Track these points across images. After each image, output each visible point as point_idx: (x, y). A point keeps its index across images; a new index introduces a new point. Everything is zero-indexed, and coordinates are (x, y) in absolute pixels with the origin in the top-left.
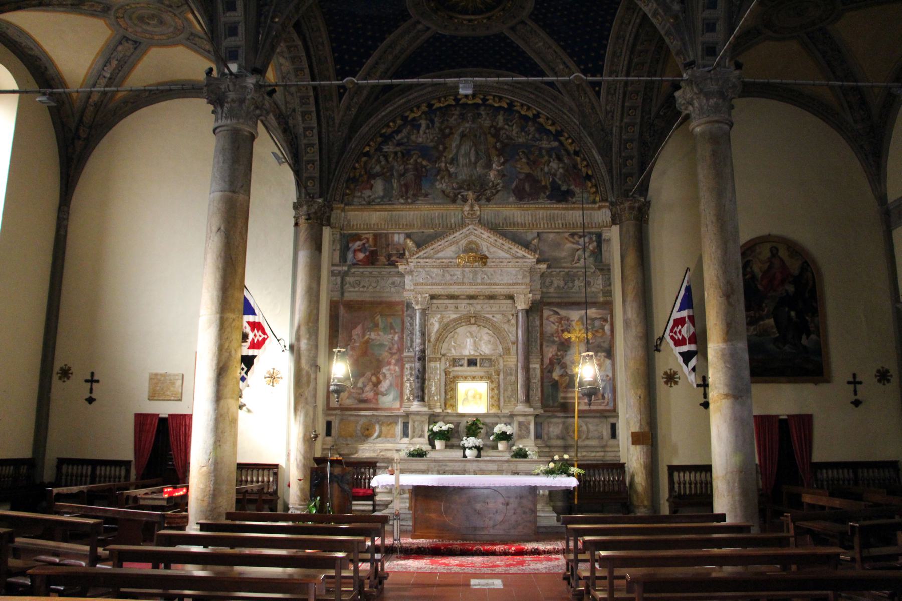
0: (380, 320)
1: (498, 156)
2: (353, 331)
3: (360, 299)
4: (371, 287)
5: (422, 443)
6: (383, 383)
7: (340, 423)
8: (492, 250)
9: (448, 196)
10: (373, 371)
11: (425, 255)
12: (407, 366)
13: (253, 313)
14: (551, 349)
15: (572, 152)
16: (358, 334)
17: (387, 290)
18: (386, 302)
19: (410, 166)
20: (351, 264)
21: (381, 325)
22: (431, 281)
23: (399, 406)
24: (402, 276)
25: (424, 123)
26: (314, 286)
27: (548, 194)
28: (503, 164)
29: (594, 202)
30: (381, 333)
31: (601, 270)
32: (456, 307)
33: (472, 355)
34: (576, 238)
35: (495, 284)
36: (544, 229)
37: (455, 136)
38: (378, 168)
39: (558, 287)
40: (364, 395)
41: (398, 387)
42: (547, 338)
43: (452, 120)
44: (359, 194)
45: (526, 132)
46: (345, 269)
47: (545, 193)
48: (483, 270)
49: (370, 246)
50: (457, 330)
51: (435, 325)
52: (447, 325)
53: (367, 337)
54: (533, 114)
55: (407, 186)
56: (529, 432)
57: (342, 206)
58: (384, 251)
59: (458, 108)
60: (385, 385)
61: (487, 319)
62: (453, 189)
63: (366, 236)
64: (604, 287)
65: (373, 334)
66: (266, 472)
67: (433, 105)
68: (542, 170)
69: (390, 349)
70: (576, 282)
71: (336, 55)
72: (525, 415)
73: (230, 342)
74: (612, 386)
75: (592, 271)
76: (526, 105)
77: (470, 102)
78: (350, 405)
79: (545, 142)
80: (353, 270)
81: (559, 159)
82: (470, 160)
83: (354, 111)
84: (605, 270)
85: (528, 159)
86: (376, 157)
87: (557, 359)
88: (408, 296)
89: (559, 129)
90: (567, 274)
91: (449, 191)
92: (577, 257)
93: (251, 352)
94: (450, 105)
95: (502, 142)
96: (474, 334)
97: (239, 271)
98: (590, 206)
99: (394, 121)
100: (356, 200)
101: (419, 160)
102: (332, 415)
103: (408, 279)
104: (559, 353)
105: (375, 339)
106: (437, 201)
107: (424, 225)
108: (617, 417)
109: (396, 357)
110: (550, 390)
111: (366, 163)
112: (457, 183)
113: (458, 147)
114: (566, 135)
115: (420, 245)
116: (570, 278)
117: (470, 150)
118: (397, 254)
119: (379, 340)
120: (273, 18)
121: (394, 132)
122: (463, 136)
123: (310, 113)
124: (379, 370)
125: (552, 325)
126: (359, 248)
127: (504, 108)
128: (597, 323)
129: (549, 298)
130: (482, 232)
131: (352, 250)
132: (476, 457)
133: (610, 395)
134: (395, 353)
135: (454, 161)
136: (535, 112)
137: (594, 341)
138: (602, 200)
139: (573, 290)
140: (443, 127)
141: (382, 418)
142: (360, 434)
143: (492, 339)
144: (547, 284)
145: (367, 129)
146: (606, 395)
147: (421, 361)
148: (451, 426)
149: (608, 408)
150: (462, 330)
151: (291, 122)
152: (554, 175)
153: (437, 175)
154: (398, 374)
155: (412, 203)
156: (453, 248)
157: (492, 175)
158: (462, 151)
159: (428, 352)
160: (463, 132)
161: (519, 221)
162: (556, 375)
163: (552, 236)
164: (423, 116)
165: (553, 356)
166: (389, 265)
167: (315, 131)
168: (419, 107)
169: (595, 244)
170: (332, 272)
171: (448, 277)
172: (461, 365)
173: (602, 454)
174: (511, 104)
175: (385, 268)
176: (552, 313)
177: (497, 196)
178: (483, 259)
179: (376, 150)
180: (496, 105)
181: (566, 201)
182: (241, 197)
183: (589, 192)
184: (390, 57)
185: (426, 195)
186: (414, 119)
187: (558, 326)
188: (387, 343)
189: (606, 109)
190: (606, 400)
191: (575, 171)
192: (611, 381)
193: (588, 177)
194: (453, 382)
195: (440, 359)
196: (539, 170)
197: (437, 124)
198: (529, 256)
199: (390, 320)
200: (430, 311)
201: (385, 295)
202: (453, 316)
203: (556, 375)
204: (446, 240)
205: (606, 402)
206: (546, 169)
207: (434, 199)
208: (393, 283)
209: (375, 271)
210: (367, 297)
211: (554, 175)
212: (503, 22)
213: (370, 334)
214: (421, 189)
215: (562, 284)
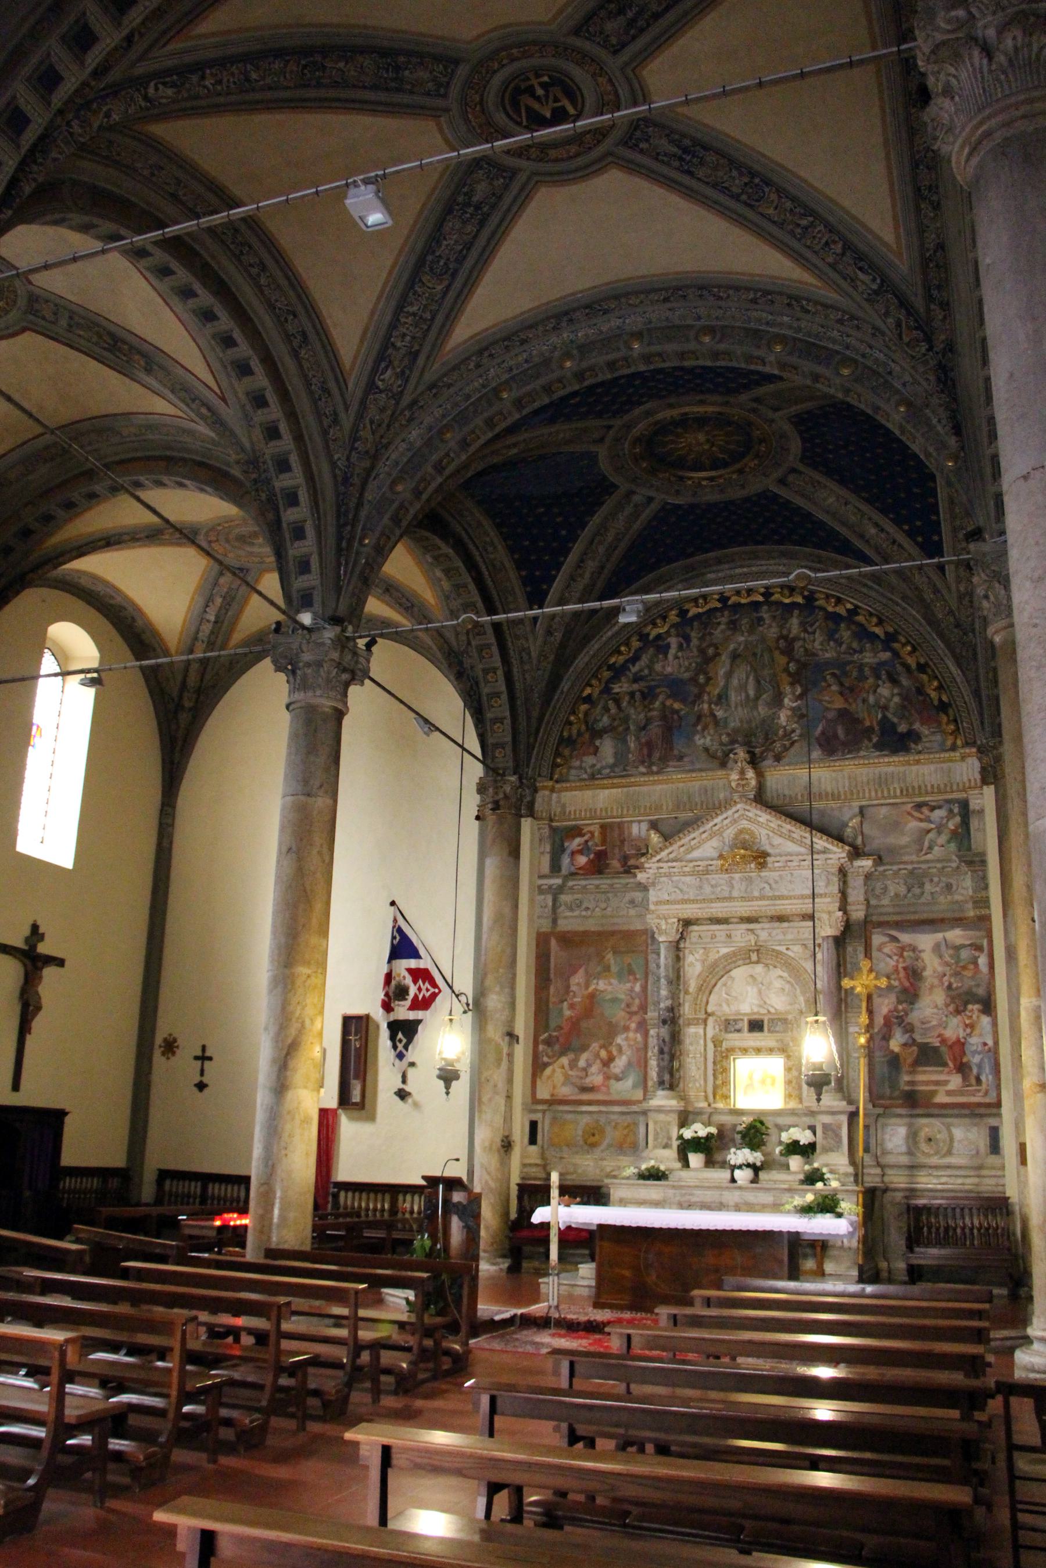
0: (612, 962)
1: (792, 684)
3: (581, 929)
5: (665, 1158)
7: (552, 1124)
8: (777, 840)
9: (713, 756)
10: (602, 1042)
11: (671, 856)
12: (652, 1032)
13: (416, 955)
14: (886, 1001)
15: (914, 666)
16: (578, 984)
18: (620, 932)
19: (655, 713)
21: (614, 969)
22: (680, 897)
24: (644, 888)
25: (673, 641)
26: (507, 910)
27: (875, 740)
28: (800, 697)
29: (954, 748)
30: (614, 981)
31: (970, 863)
32: (729, 936)
33: (758, 1013)
34: (925, 810)
35: (780, 897)
36: (870, 799)
37: (723, 657)
38: (605, 720)
39: (897, 895)
43: (718, 633)
44: (577, 763)
45: (836, 641)
46: (558, 881)
47: (870, 740)
48: (763, 874)
50: (733, 973)
51: (694, 965)
52: (715, 965)
53: (592, 988)
54: (848, 610)
55: (649, 745)
56: (840, 1141)
57: (550, 783)
58: (617, 851)
59: (726, 613)
60: (619, 1064)
61: (779, 953)
62: (722, 744)
64: (974, 891)
66: (372, 1195)
67: (688, 611)
68: (864, 701)
69: (628, 1006)
70: (928, 887)
71: (516, 556)
72: (833, 1113)
73: (303, 1009)
75: (954, 865)
76: (833, 596)
77: (743, 601)
79: (868, 654)
80: (570, 883)
81: (894, 681)
82: (747, 696)
83: (558, 636)
84: (976, 862)
85: (841, 684)
86: (602, 702)
88: (652, 921)
89: (890, 630)
90: (912, 872)
91: (714, 748)
92: (926, 844)
93: (412, 1015)
94: (716, 609)
95: (798, 661)
96: (760, 979)
97: (318, 906)
98: (947, 755)
99: (627, 644)
100: (573, 772)
101: (668, 703)
102: (535, 1111)
103: (653, 895)
104: (900, 1007)
106: (698, 766)
107: (678, 806)
108: (999, 1115)
109: (636, 1018)
111: (586, 714)
112: (728, 735)
113: (729, 675)
114: (903, 640)
115: (667, 838)
116: (916, 879)
117: (747, 678)
120: (362, 539)
121: (627, 661)
122: (735, 656)
123: (488, 646)
127: (799, 604)
128: (965, 954)
129: (881, 914)
130: (759, 812)
131: (568, 851)
132: (752, 1182)
134: (636, 1013)
135: (722, 699)
136: (849, 606)
138: (967, 744)
139: (923, 900)
140: (704, 645)
141: (613, 1117)
142: (581, 1143)
143: (787, 987)
144: (878, 891)
145: (586, 659)
146: (983, 1078)
148: (713, 1130)
149: (987, 1100)
150: (740, 973)
151: (467, 662)
152: (885, 708)
153: (695, 725)
154: (641, 1046)
155: (658, 773)
156: (715, 843)
157: (783, 717)
158: (735, 682)
159: (687, 1010)
160: (735, 650)
161: (829, 789)
162: (895, 1045)
163: (884, 810)
164: (672, 630)
167: (500, 673)
168: (664, 618)
169: (958, 819)
170: (539, 887)
171: (708, 889)
172: (739, 1031)
173: (976, 1180)
174: (810, 599)
176: (887, 939)
177: (792, 751)
178: (761, 858)
179: (601, 692)
180: (787, 601)
181: (907, 750)
182: (321, 802)
183: (943, 732)
184: (601, 549)
185: (680, 758)
186: (659, 637)
188: (623, 996)
189: (958, 590)
190: (984, 1087)
191: (921, 698)
193: (943, 707)
194: (727, 1057)
195: (705, 1021)
196: (859, 701)
197: (695, 642)
198: (835, 849)
199: (628, 959)
200: (687, 945)
202: (724, 951)
203: (895, 1045)
204: (702, 830)
206: (871, 699)
207: (692, 763)
209: (604, 882)
210: (591, 925)
211: (885, 708)
212: (764, 474)
214: (671, 749)
215: (902, 890)
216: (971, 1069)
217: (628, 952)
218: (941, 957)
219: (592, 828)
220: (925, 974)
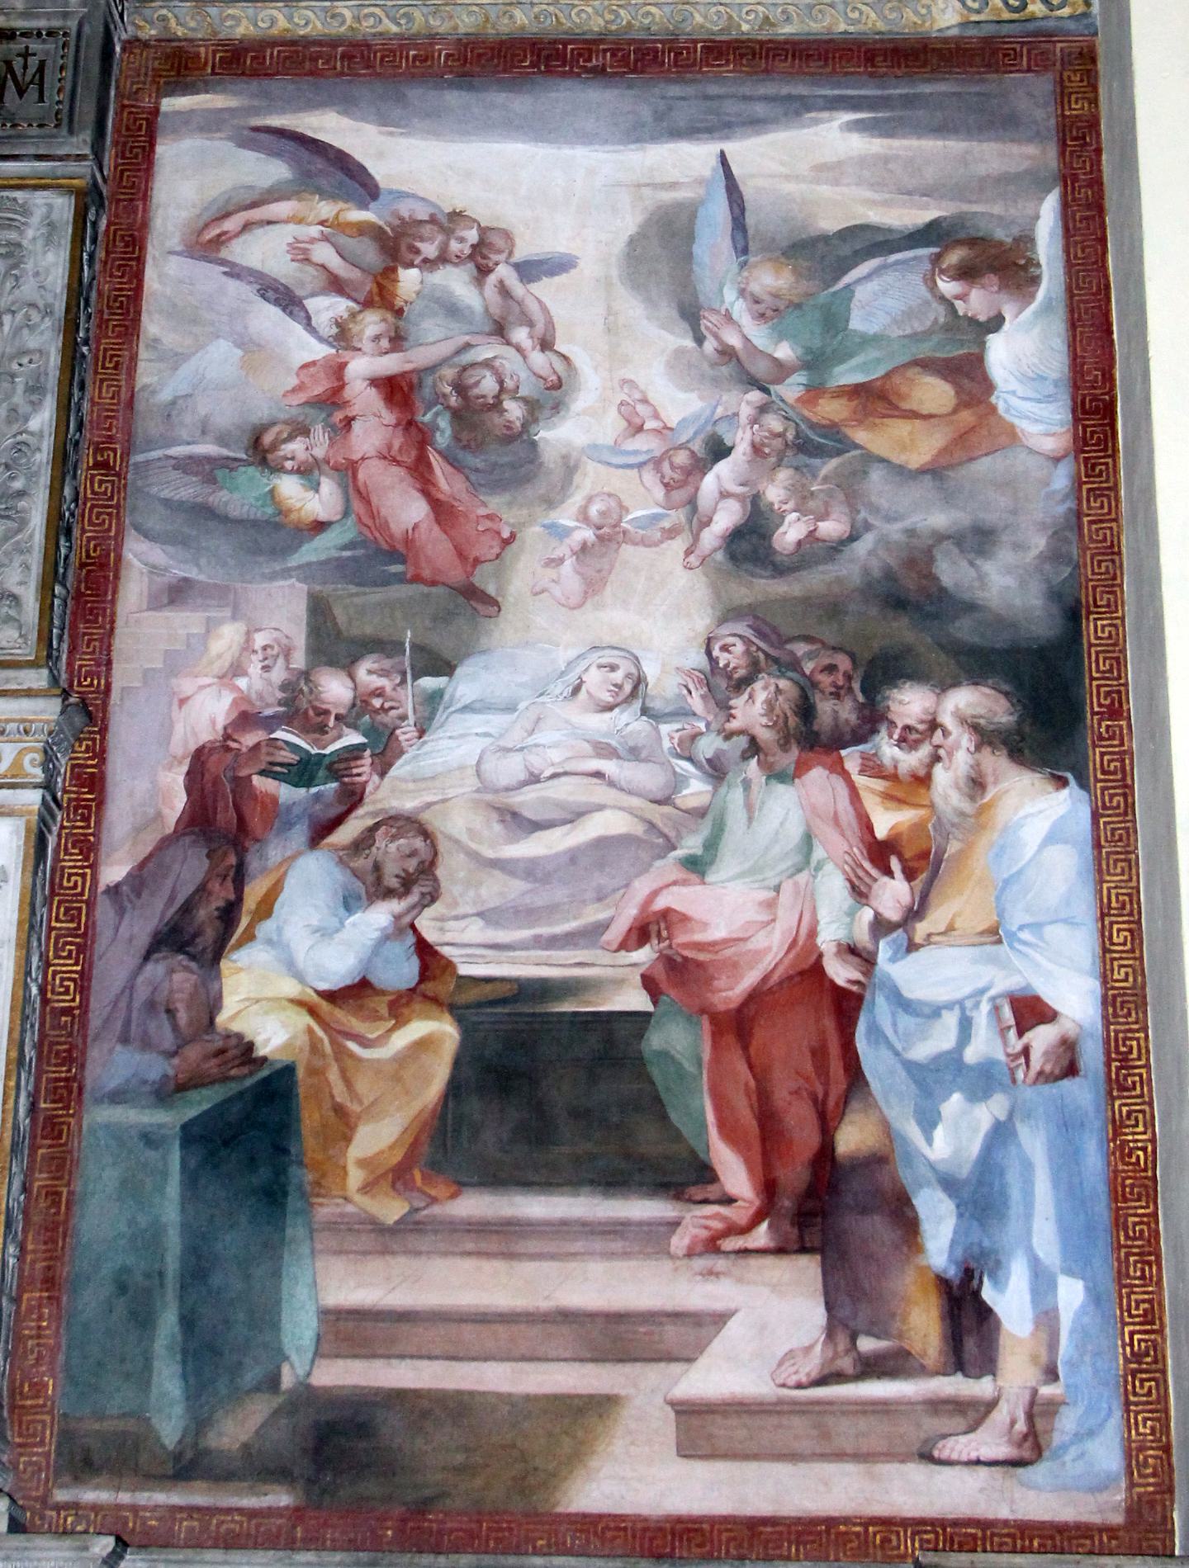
14: (228, 637)
42: (187, 490)
74: (1094, 1159)
87: (303, 771)
104: (335, 689)
110: (169, 1207)
125: (268, 318)
133: (1071, 1294)
137: (831, 528)
165: (245, 719)
176: (275, 170)
187: (343, 336)
192: (1083, 1093)
205: (1010, 1412)
216: (908, 1224)
218: (691, 314)
220: (556, 436)
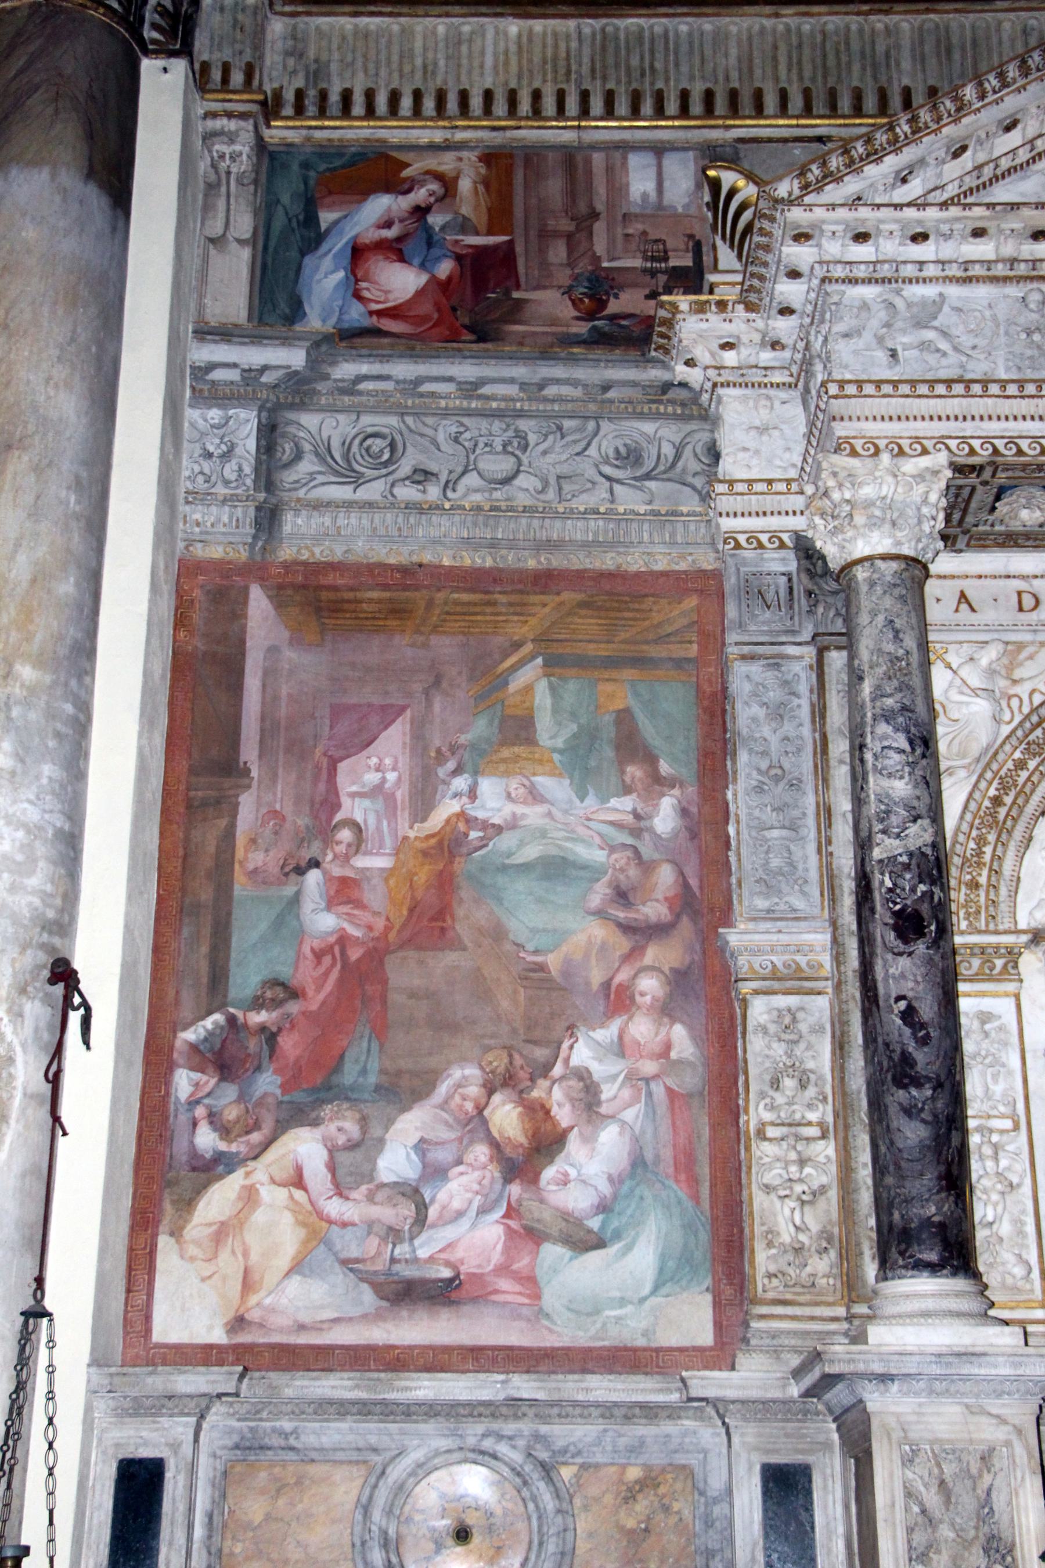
0: (542, 697)
2: (343, 767)
4: (472, 480)
6: (573, 1144)
10: (499, 1061)
16: (377, 790)
17: (580, 503)
20: (329, 328)
23: (706, 1337)
40: (426, 1246)
41: (693, 1181)
46: (295, 358)
49: (465, 226)
53: (447, 808)
63: (431, 162)
65: (487, 786)
69: (622, 896)
78: (317, 1327)
80: (346, 370)
105: (513, 824)
118: (653, 273)
119: (543, 833)
124: (540, 1053)
126: (390, 233)
131: (338, 244)
147: (920, 947)
154: (691, 1081)
166: (600, 340)
170: (201, 372)
175: (573, 360)
201: (575, 530)
208: (631, 456)
213: (473, 794)
217: (613, 663)
219: (446, 163)
